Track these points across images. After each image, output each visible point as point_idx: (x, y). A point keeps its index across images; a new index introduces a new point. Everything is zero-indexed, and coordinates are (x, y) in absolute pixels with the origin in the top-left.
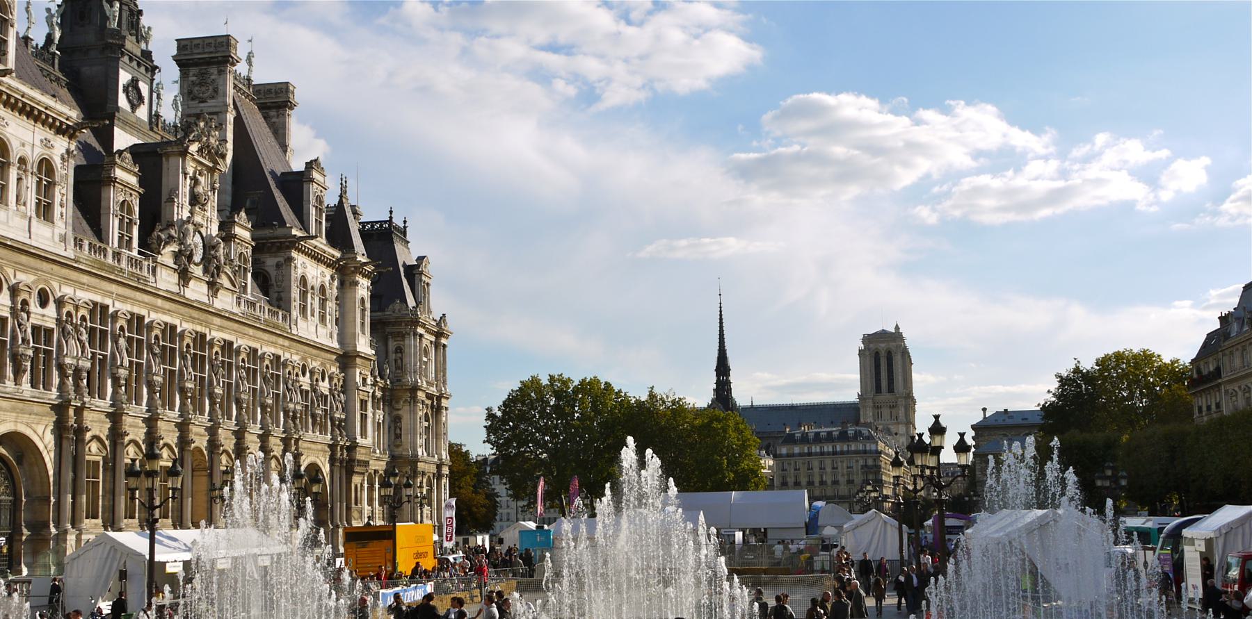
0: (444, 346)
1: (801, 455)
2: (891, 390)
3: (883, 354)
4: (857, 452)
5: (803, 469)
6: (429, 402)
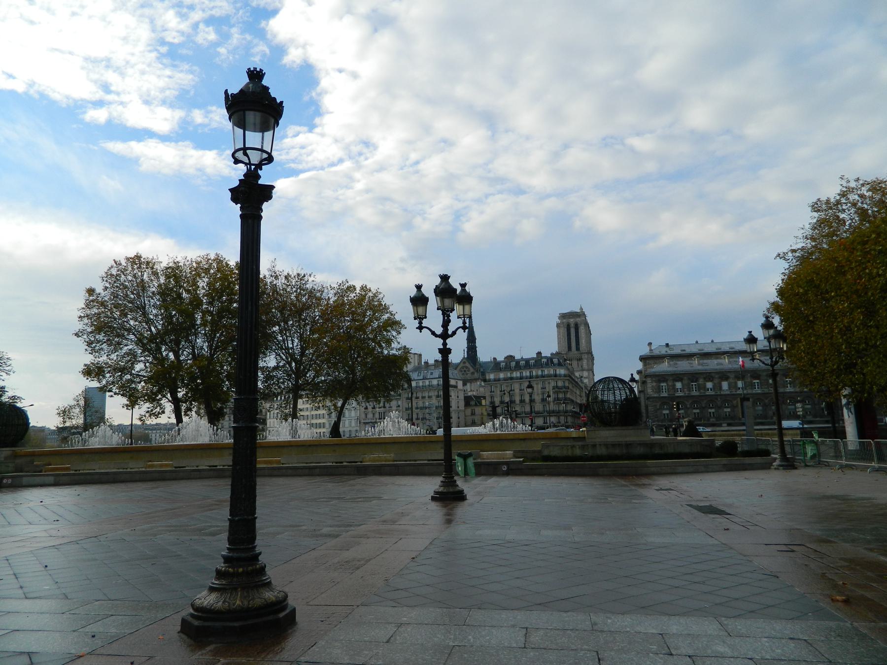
1: (505, 379)
2: (578, 349)
3: (572, 325)
4: (549, 376)
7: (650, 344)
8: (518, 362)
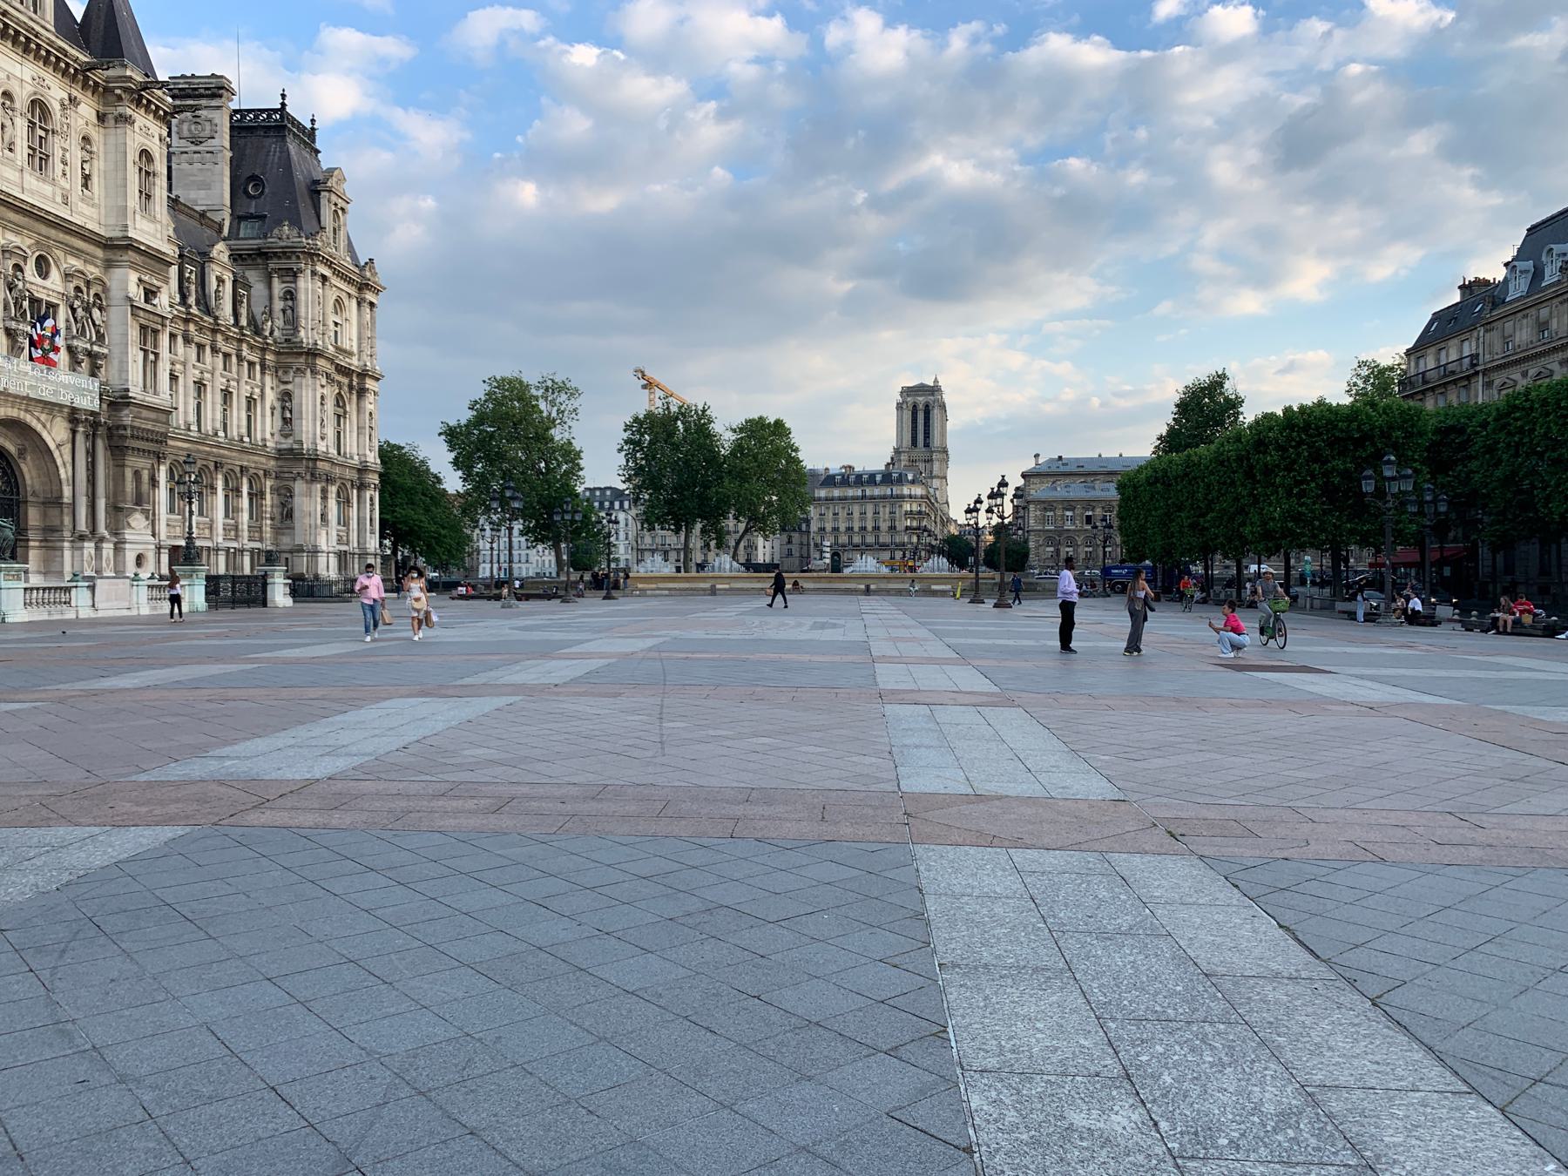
0: (372, 304)
1: (840, 499)
2: (927, 445)
5: (843, 514)
6: (345, 381)
7: (1037, 456)
8: (859, 476)
